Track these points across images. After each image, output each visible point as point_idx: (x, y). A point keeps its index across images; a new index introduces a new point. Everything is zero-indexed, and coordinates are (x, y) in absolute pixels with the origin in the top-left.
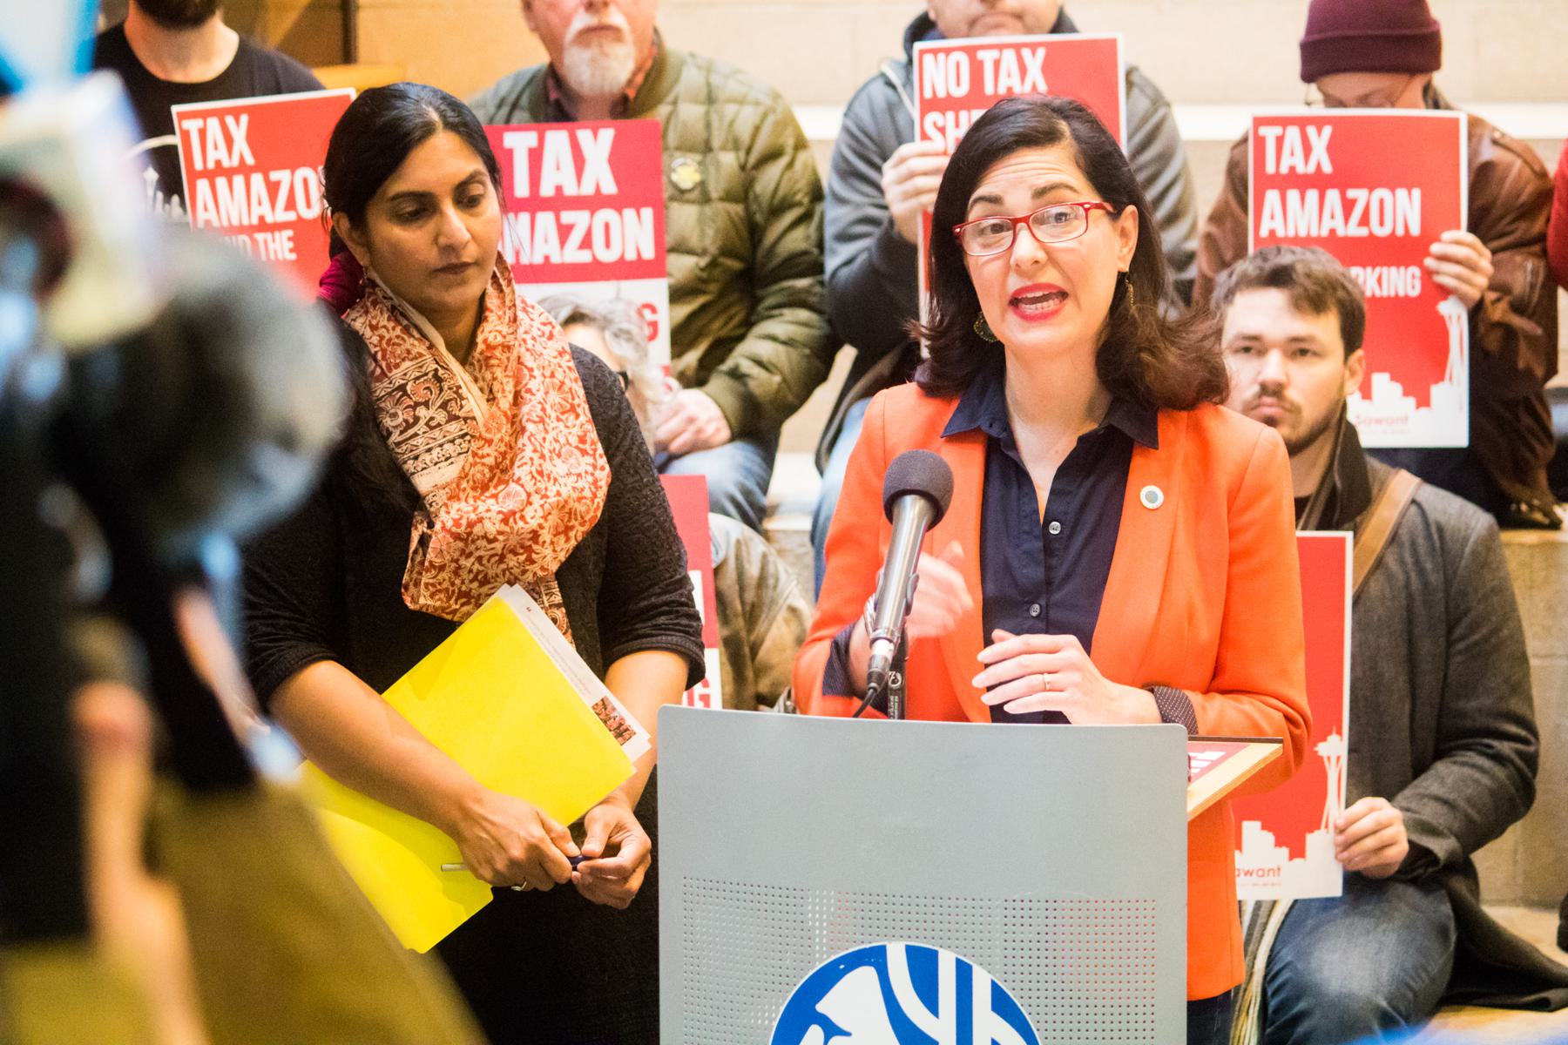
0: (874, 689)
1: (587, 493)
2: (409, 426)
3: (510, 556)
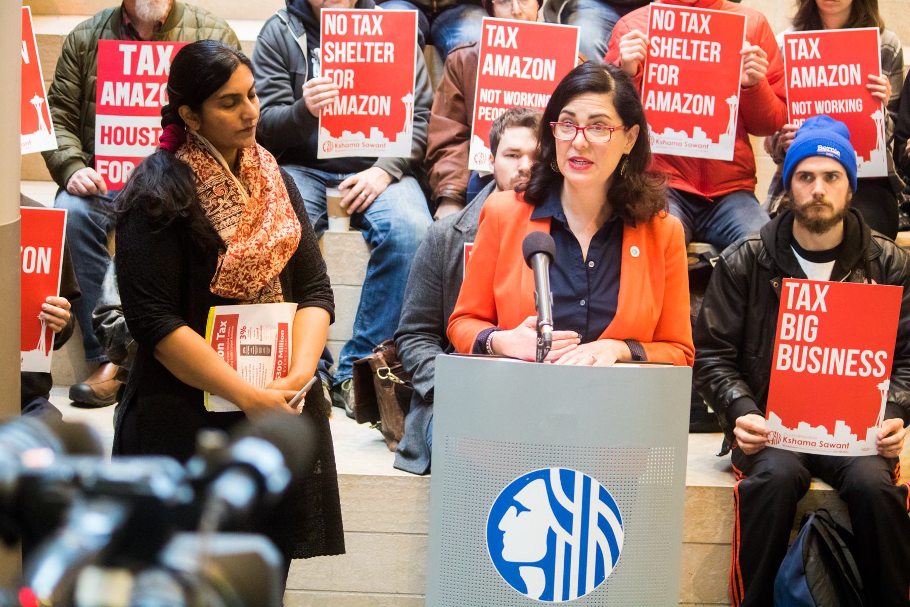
1: (294, 236)
2: (215, 208)
3: (261, 266)
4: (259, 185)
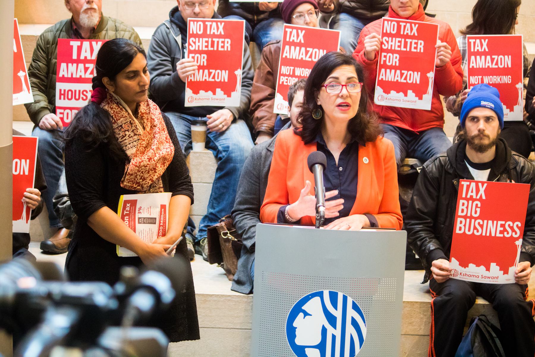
0: (323, 220)
2: (124, 137)
3: (150, 171)
4: (150, 124)
